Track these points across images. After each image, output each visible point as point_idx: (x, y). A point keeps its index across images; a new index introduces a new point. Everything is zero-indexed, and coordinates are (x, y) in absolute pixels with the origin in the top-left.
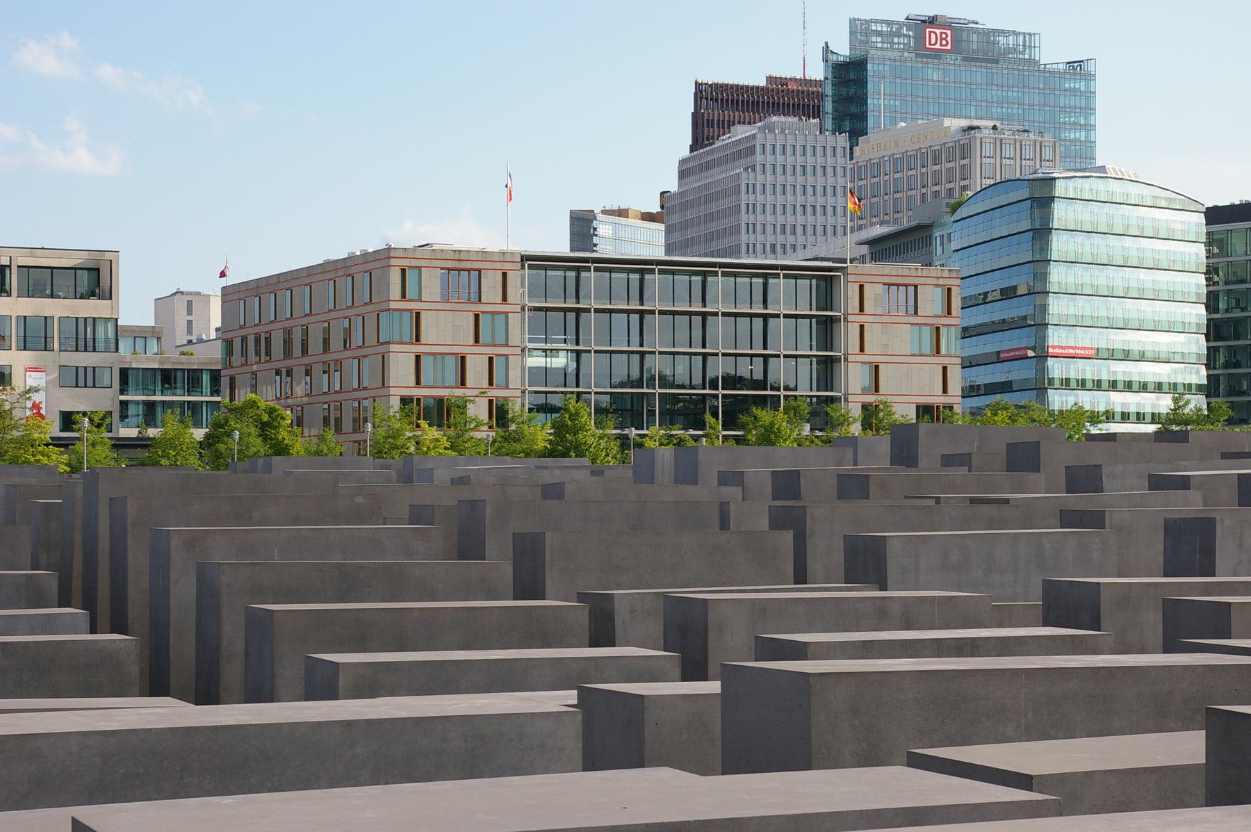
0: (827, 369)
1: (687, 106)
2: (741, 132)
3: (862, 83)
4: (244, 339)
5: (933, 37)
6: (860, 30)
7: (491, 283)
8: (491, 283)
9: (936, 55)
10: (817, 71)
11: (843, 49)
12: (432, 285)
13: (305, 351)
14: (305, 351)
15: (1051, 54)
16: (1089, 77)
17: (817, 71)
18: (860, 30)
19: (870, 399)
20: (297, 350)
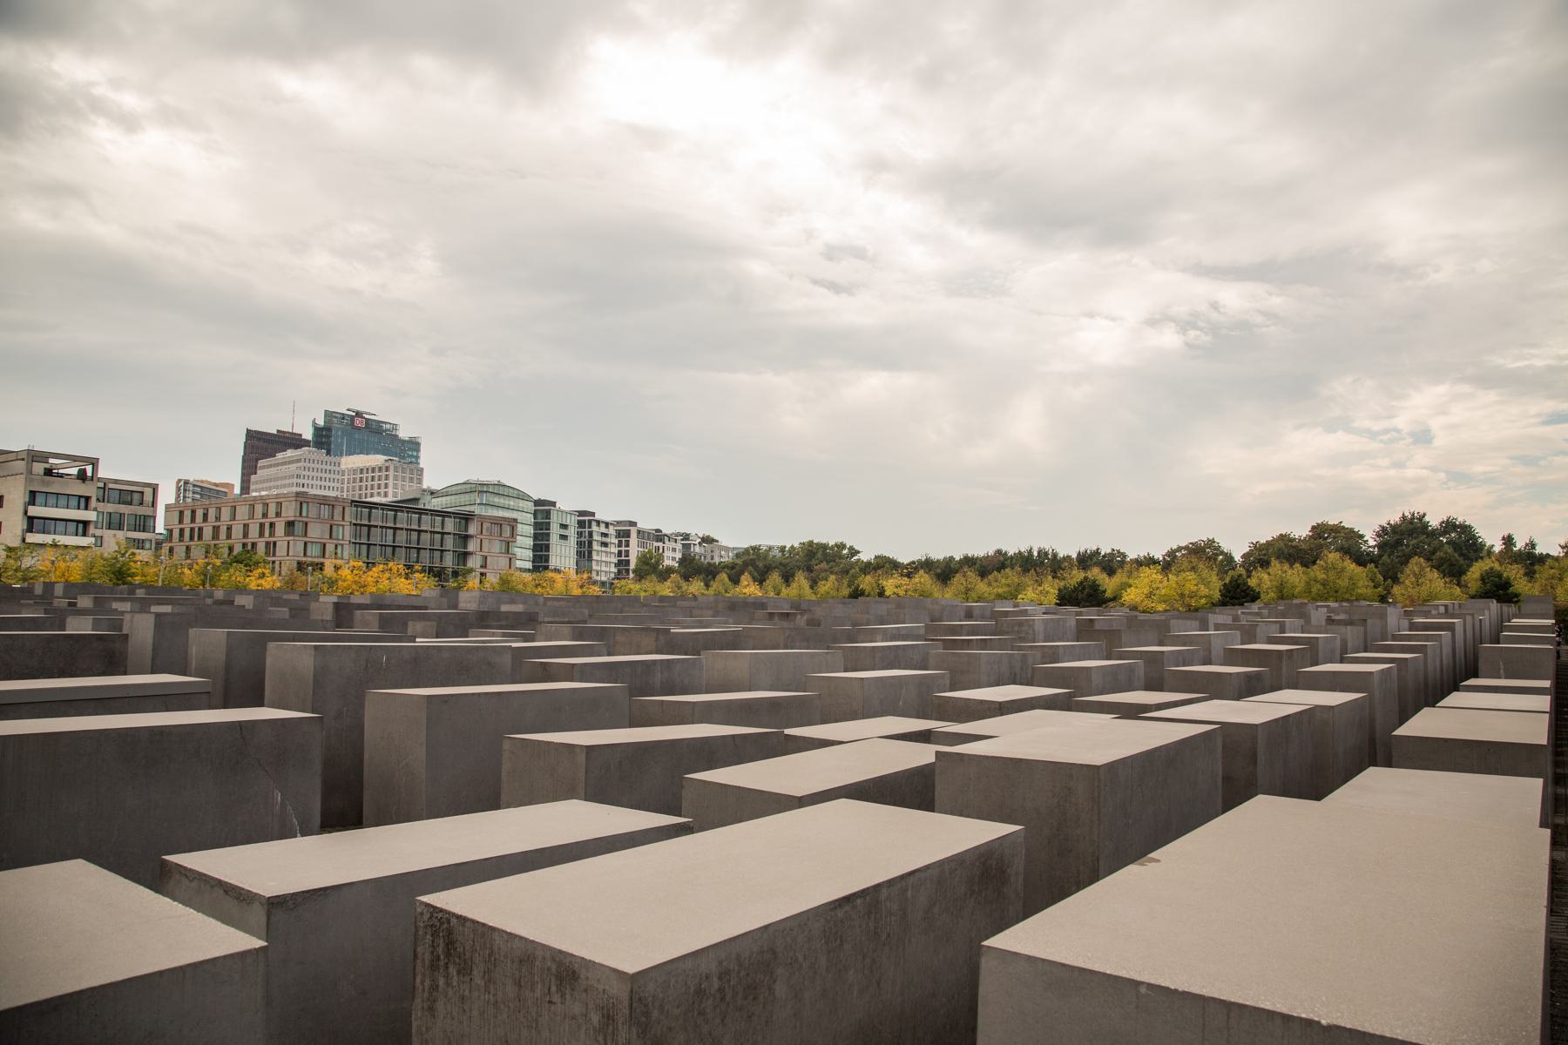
0: (464, 556)
2: (290, 453)
3: (329, 437)
4: (182, 530)
5: (358, 422)
6: (329, 414)
7: (338, 511)
8: (338, 511)
9: (359, 429)
11: (321, 422)
12: (313, 512)
13: (229, 536)
14: (229, 536)
15: (403, 434)
16: (418, 444)
18: (329, 414)
20: (223, 535)
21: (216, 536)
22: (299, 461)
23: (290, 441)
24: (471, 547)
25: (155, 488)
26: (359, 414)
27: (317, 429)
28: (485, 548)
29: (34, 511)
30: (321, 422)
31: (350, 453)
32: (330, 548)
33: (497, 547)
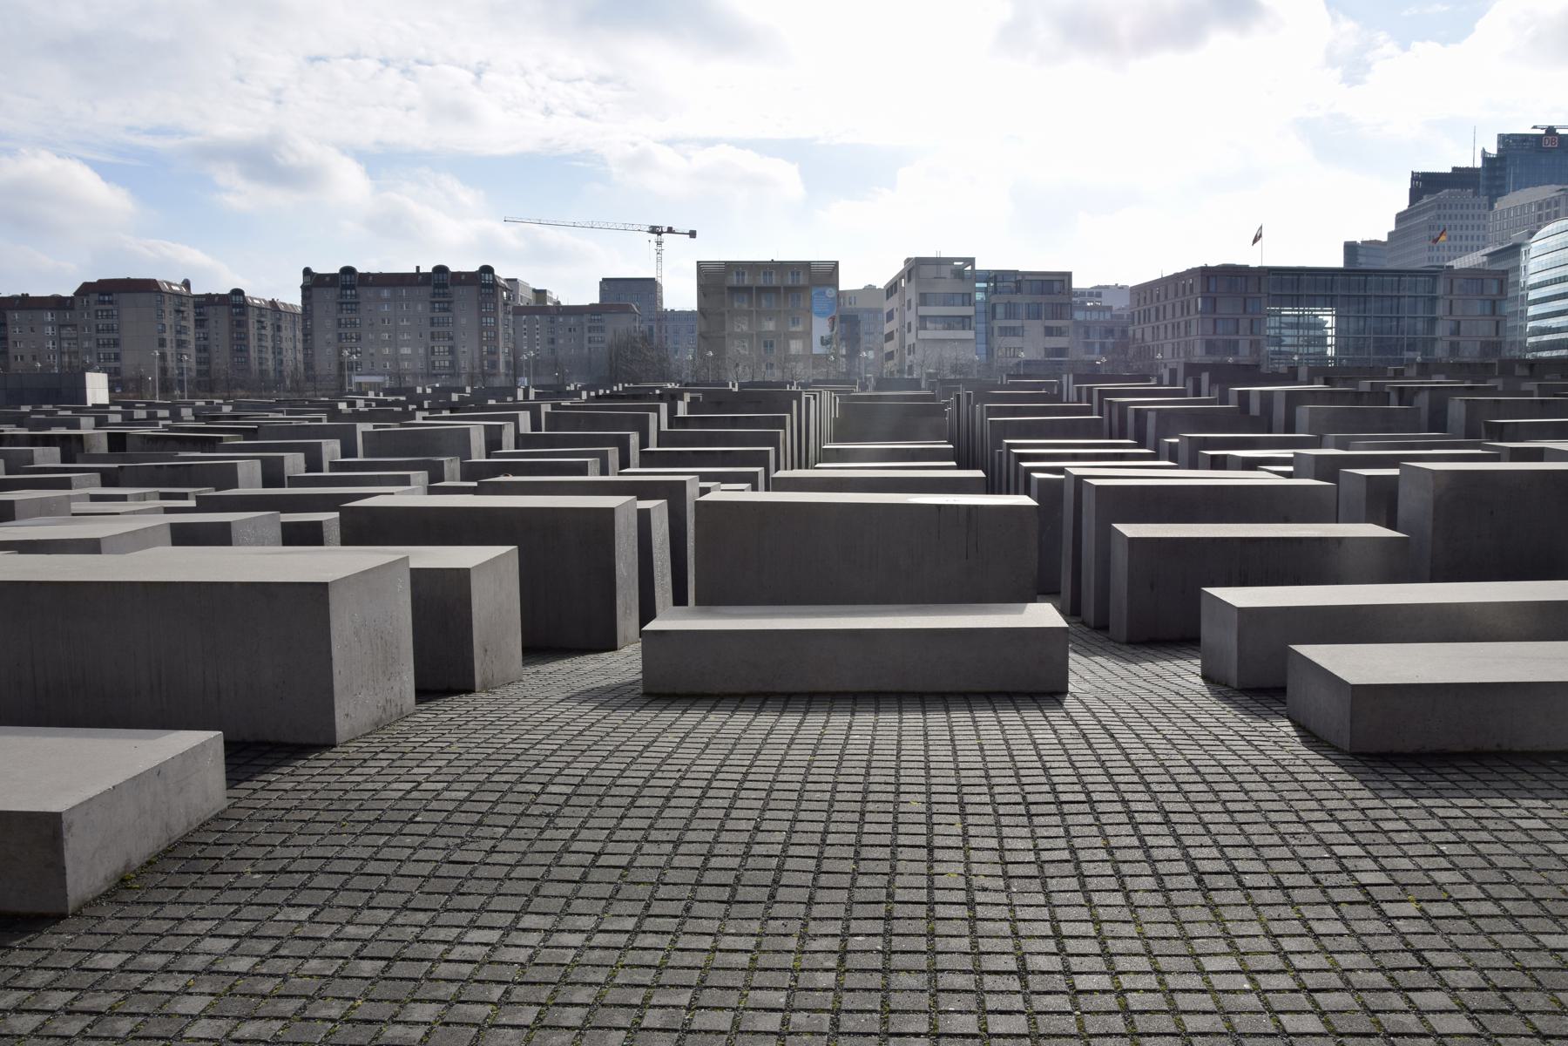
0: (1432, 321)
1: (1406, 185)
5: (1547, 144)
6: (1504, 140)
9: (1549, 150)
10: (1479, 164)
11: (1493, 150)
17: (1479, 164)
18: (1504, 140)
19: (1455, 339)
21: (1157, 318)
22: (1432, 209)
23: (1460, 178)
24: (1441, 309)
25: (1069, 275)
26: (1551, 131)
27: (1486, 159)
28: (1457, 311)
29: (924, 311)
30: (1493, 150)
31: (1519, 186)
32: (1244, 324)
33: (1477, 308)
